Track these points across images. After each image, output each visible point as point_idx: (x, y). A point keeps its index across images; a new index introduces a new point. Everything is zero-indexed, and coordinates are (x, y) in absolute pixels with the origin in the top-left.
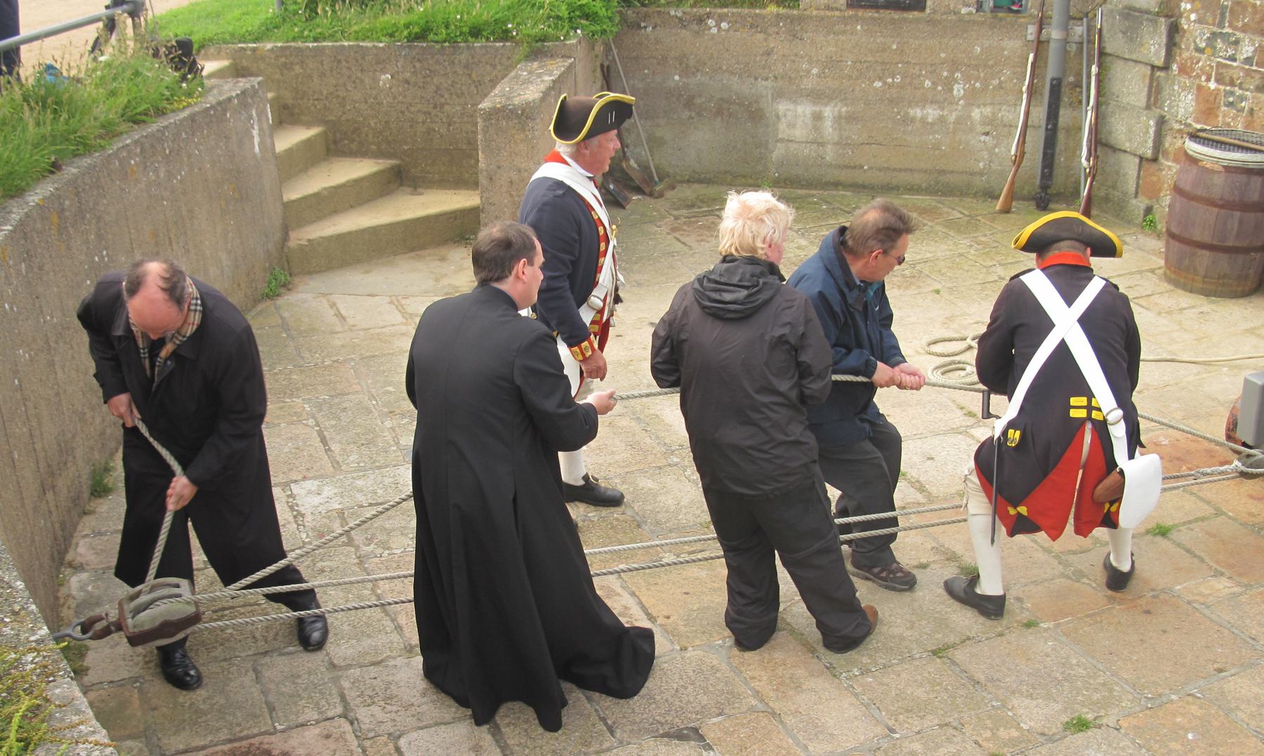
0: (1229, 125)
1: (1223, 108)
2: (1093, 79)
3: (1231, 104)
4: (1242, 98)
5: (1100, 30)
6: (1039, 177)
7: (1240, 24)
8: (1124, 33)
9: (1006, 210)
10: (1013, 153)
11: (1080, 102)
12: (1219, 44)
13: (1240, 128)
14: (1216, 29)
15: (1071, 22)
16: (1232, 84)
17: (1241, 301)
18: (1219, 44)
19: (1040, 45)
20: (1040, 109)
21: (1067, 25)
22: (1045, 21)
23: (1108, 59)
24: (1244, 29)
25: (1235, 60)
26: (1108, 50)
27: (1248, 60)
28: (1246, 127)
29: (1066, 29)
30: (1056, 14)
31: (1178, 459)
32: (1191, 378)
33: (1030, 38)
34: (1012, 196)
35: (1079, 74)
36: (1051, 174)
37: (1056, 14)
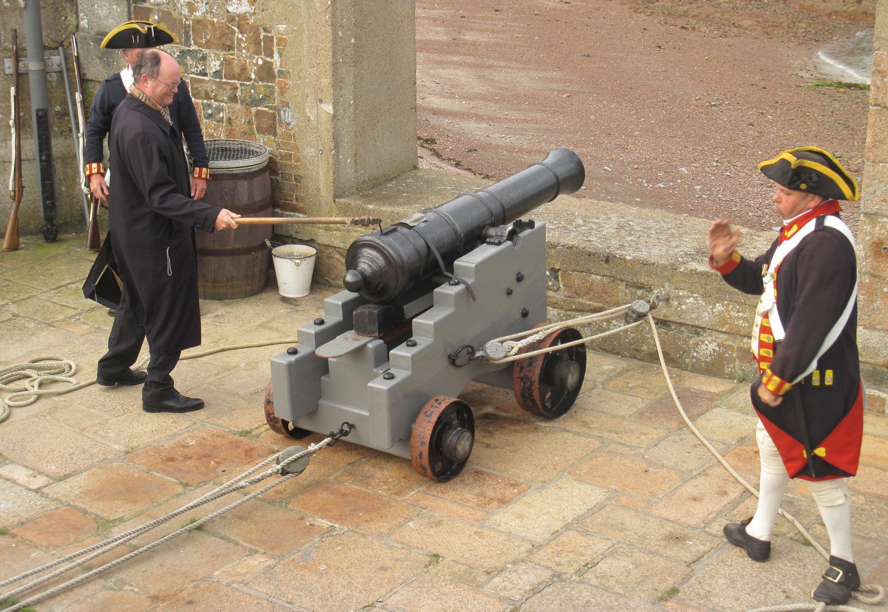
0: (212, 135)
1: (205, 121)
2: (79, 105)
3: (210, 116)
4: (219, 110)
5: (78, 57)
6: (42, 209)
7: (204, 41)
8: (101, 58)
9: (14, 247)
10: (11, 189)
11: (71, 130)
12: (190, 61)
13: (223, 137)
14: (183, 47)
15: (47, 52)
16: (208, 97)
17: (252, 299)
18: (190, 61)
19: (20, 78)
20: (32, 141)
21: (43, 55)
22: (20, 53)
23: (91, 85)
24: (208, 45)
25: (205, 75)
26: (89, 76)
27: (217, 74)
28: (227, 136)
29: (42, 59)
30: (29, 44)
31: (205, 456)
32: (211, 379)
33: (8, 71)
34: (18, 232)
35: (64, 103)
36: (53, 204)
37: (29, 44)
